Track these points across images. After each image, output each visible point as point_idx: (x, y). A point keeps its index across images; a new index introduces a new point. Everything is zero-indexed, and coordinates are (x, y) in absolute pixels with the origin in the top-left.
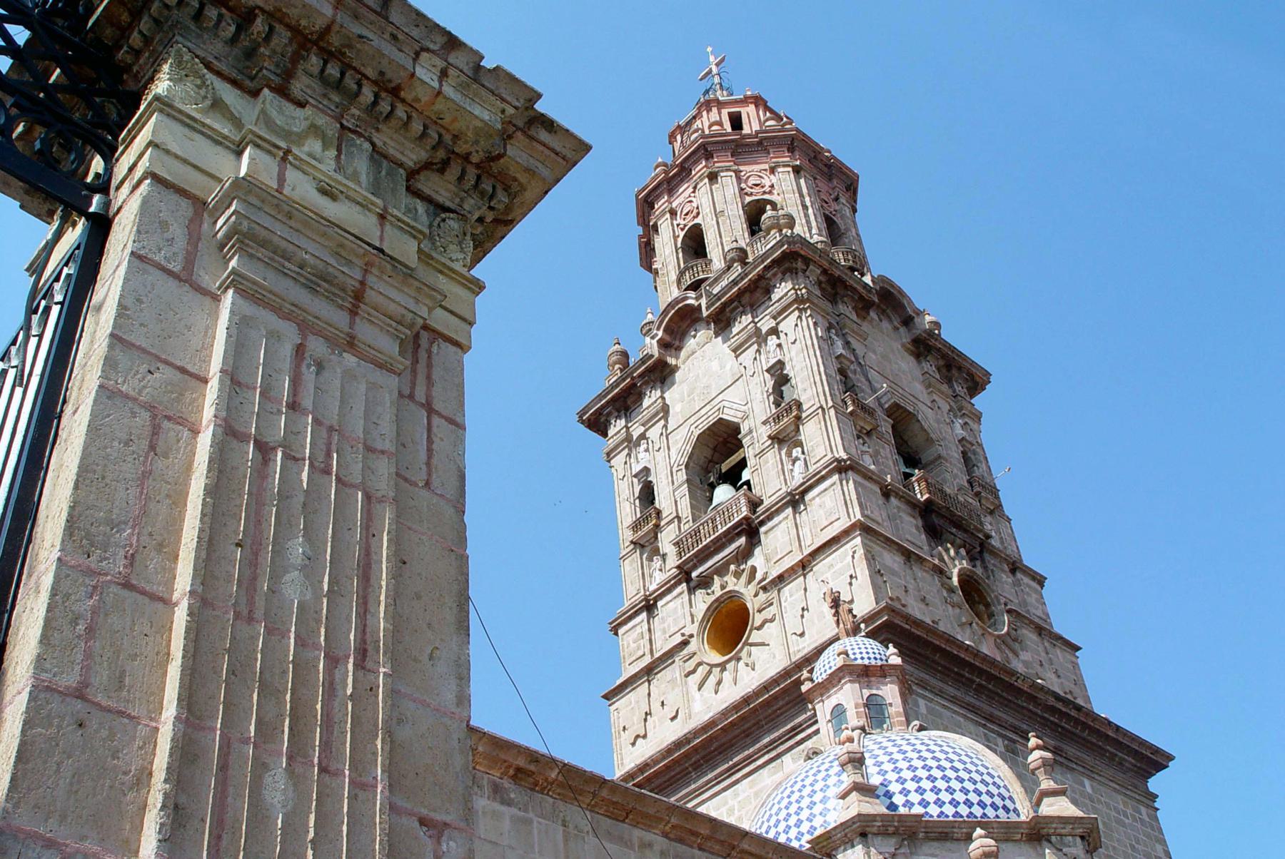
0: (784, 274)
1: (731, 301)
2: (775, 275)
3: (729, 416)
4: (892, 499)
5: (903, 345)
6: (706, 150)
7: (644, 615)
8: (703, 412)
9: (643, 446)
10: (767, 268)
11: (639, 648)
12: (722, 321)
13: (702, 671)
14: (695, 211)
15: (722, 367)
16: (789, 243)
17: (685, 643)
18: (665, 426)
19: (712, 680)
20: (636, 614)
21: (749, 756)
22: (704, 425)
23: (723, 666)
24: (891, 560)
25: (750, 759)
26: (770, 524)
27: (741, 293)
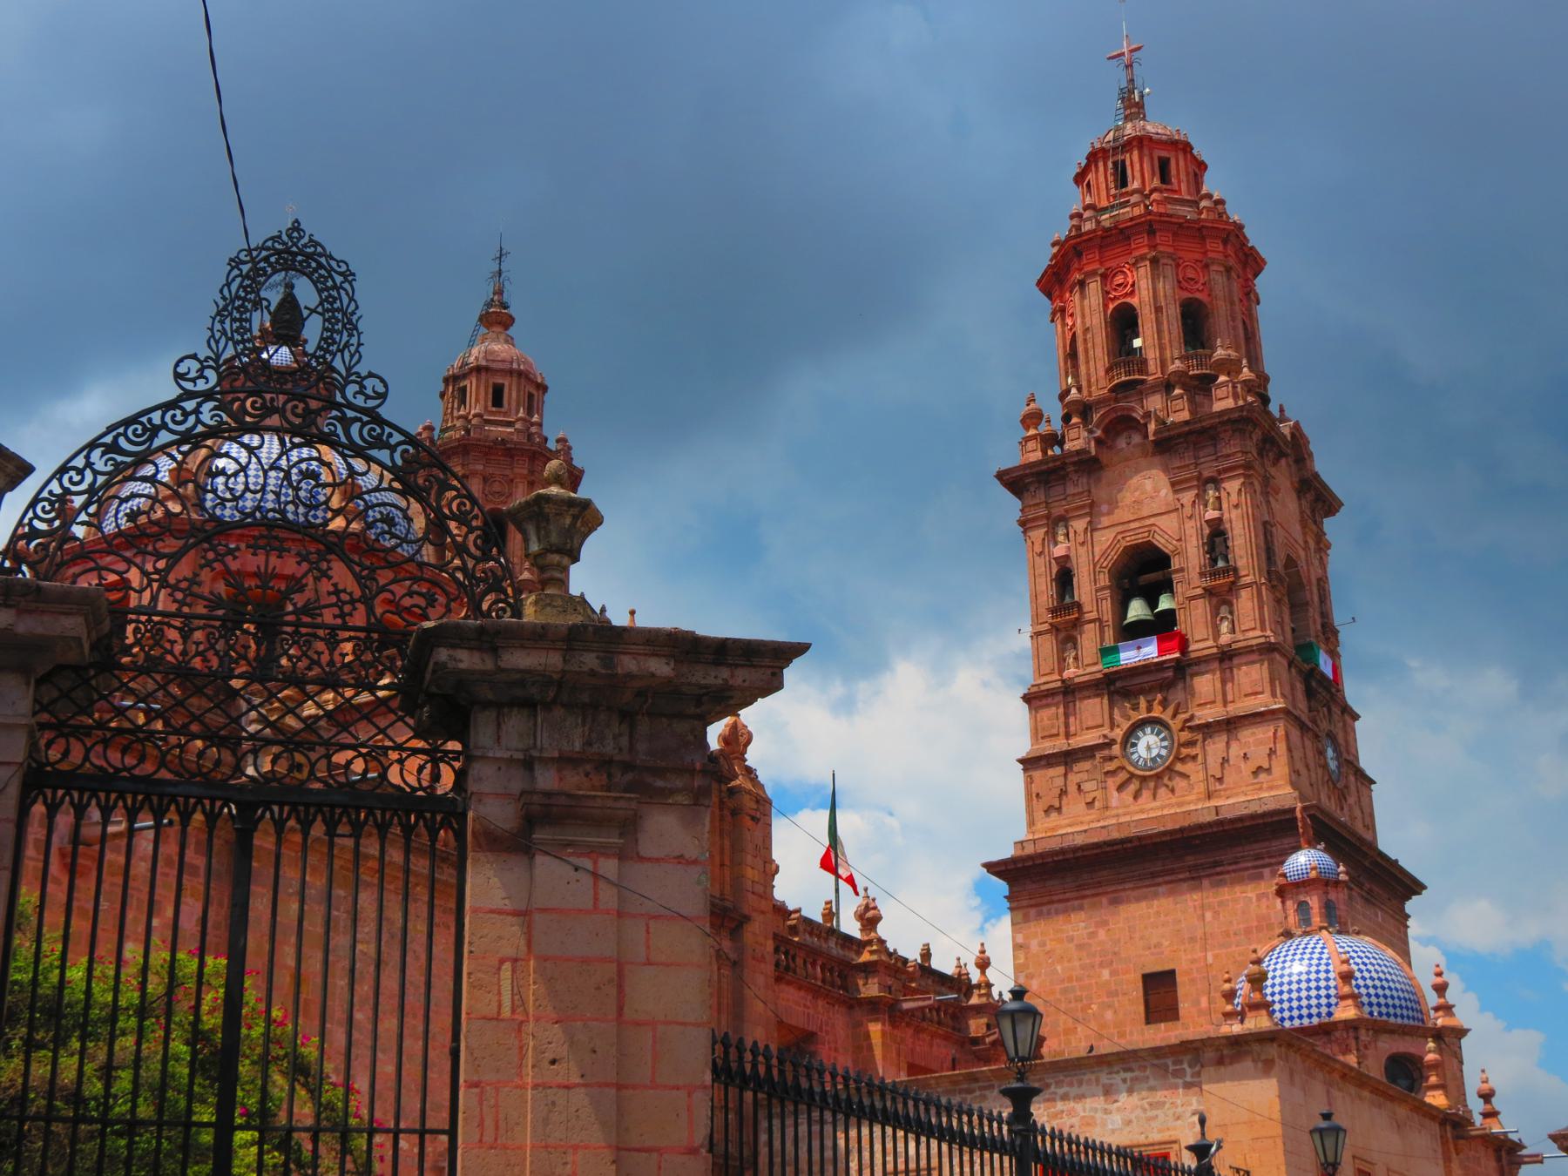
0: (1234, 431)
1: (1179, 435)
2: (1225, 431)
3: (1160, 541)
5: (1292, 483)
6: (1151, 226)
7: (1059, 698)
8: (1133, 525)
9: (1061, 531)
11: (1053, 727)
13: (1123, 776)
14: (1128, 289)
15: (1157, 491)
16: (1248, 411)
17: (1109, 744)
19: (1133, 787)
20: (1053, 694)
21: (1173, 869)
22: (1131, 540)
23: (1144, 779)
24: (1295, 734)
25: (1172, 872)
27: (1190, 433)
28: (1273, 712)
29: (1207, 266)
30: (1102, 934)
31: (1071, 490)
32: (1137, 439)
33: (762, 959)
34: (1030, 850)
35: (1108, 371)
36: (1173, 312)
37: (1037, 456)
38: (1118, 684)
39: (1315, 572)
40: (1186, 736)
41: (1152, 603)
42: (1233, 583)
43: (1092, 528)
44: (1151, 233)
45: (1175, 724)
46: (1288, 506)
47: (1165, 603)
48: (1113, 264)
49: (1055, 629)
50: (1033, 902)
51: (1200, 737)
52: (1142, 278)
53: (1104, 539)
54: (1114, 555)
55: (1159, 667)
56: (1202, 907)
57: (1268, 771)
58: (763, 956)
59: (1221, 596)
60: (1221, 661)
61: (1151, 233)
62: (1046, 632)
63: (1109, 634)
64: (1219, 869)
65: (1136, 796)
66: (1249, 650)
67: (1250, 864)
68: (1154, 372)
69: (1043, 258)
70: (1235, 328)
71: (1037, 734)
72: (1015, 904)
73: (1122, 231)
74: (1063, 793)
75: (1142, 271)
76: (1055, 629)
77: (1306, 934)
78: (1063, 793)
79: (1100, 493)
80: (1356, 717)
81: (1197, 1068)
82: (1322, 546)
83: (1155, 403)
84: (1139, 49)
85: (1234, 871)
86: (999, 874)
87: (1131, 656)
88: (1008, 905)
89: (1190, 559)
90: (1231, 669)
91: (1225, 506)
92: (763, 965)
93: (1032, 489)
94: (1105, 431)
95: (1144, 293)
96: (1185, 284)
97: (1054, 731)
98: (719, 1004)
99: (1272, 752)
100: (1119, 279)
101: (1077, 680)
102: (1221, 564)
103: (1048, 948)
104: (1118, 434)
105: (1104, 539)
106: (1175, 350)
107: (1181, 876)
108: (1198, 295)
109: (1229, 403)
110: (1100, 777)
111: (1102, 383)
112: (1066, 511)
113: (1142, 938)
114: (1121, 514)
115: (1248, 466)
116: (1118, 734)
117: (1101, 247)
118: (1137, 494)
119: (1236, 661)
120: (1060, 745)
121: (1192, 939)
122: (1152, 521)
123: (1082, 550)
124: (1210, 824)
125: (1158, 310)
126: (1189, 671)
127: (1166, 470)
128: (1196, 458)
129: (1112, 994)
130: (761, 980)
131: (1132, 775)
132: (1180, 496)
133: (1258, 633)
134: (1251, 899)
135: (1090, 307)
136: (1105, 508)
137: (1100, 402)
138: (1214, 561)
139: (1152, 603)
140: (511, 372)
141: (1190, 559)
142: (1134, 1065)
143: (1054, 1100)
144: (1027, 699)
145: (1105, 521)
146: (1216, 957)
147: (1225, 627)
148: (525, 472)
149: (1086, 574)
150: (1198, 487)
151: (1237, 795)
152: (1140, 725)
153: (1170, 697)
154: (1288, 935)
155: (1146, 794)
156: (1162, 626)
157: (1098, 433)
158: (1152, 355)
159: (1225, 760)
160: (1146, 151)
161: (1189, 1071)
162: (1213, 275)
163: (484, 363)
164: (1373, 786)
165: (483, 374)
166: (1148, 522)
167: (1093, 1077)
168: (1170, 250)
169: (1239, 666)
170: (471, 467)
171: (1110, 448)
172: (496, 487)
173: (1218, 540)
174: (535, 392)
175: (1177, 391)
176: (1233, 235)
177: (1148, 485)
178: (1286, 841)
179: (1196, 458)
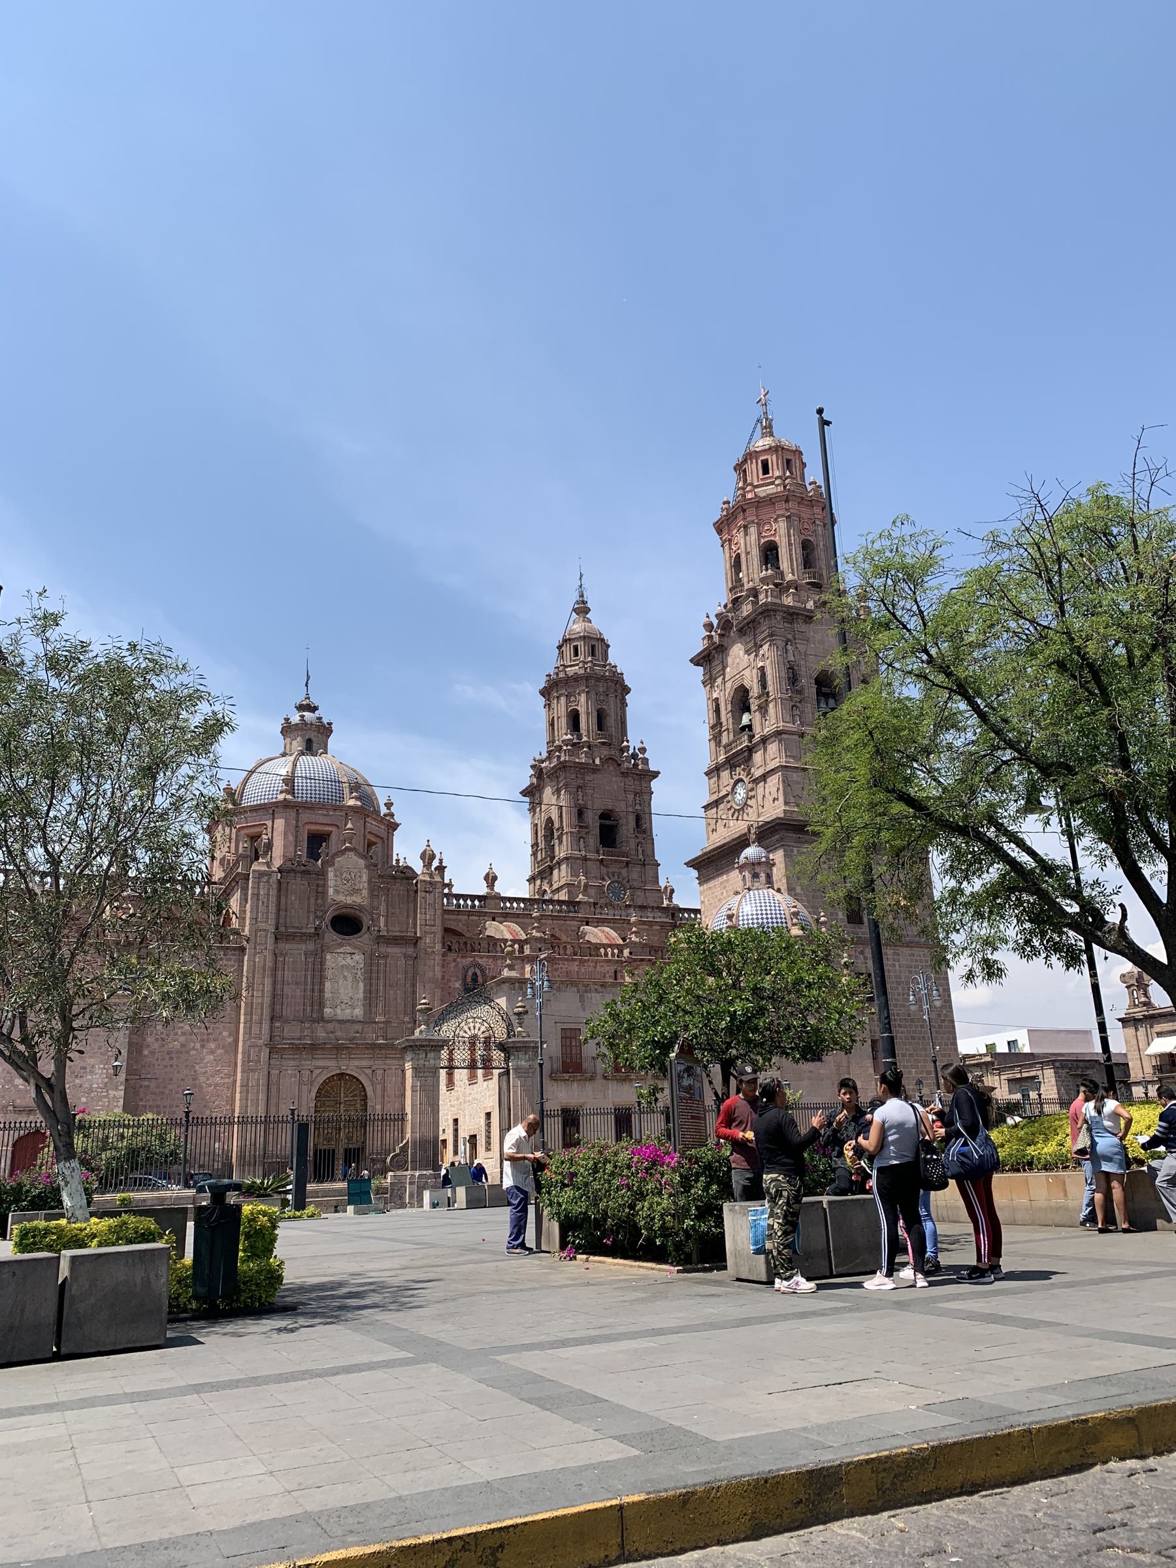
3: (747, 684)
12: (742, 631)
13: (733, 810)
17: (727, 795)
18: (724, 679)
23: (739, 811)
27: (748, 624)
36: (755, 552)
43: (724, 682)
44: (744, 511)
89: (755, 690)
99: (778, 789)
108: (773, 538)
125: (747, 553)
141: (755, 690)
158: (745, 580)
159: (764, 796)
174: (596, 643)
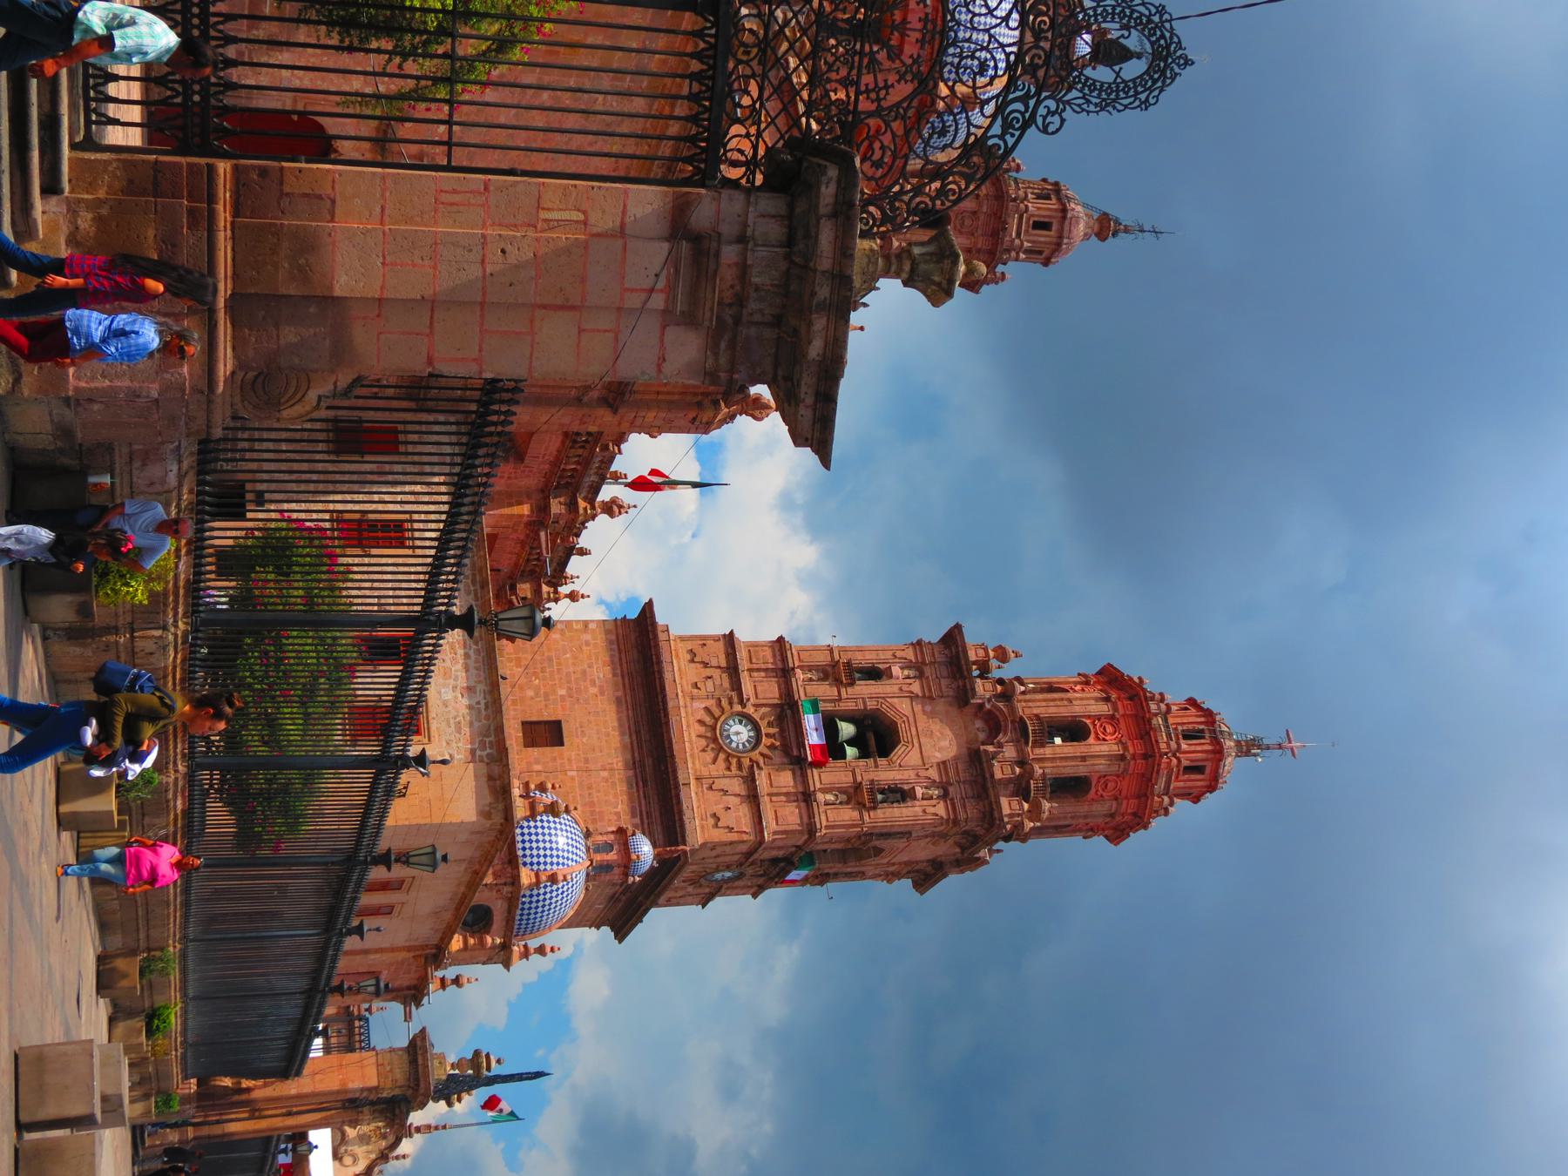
0: (983, 813)
1: (982, 770)
2: (984, 806)
3: (899, 750)
4: (794, 849)
6: (1151, 756)
7: (780, 665)
8: (913, 729)
9: (912, 673)
10: (991, 804)
11: (758, 659)
13: (717, 712)
14: (1101, 736)
15: (940, 750)
17: (742, 702)
19: (708, 720)
22: (902, 727)
23: (714, 728)
24: (744, 848)
25: (640, 748)
26: (798, 773)
28: (762, 832)
29: (1116, 799)
30: (594, 690)
31: (944, 682)
32: (982, 736)
33: (582, 422)
34: (662, 636)
35: (1037, 716)
36: (1081, 770)
37: (972, 656)
38: (789, 712)
39: (870, 871)
40: (746, 762)
41: (851, 742)
42: (864, 806)
43: (913, 697)
44: (1145, 756)
45: (755, 755)
46: (922, 852)
47: (851, 752)
48: (1122, 725)
49: (835, 664)
50: (621, 637)
51: (745, 774)
52: (1110, 747)
53: (904, 706)
54: (891, 714)
55: (801, 745)
56: (611, 769)
57: (716, 826)
58: (584, 423)
59: (855, 795)
60: (803, 794)
61: (1145, 756)
62: (832, 657)
63: (829, 707)
64: (641, 784)
65: (701, 722)
66: (811, 816)
67: (644, 809)
68: (1033, 752)
69: (1131, 670)
70: (1065, 818)
71: (753, 647)
72: (619, 623)
73: (1148, 733)
74: (706, 665)
75: (1115, 747)
76: (835, 664)
77: (588, 849)
78: (706, 665)
79: (941, 706)
80: (755, 896)
81: (485, 759)
82: (890, 877)
83: (1010, 752)
84: (1294, 755)
85: (639, 796)
86: (644, 609)
87: (810, 722)
88: (619, 618)
89: (885, 773)
90: (797, 801)
91: (925, 802)
92: (578, 422)
93: (946, 652)
94: (990, 712)
95: (1097, 748)
96: (1102, 781)
97: (754, 661)
98: (548, 386)
99: (731, 829)
100: (1109, 729)
101: (793, 680)
102: (880, 797)
103: (584, 648)
104: (987, 722)
105: (904, 706)
106: (1051, 770)
107: (636, 755)
108: (1093, 790)
109: (1006, 810)
110: (717, 694)
111: (1028, 711)
112: (928, 678)
113: (590, 722)
114: (922, 720)
115: (956, 822)
116: (750, 710)
117: (1136, 716)
118: (938, 734)
119: (803, 805)
120: (743, 664)
121: (587, 761)
122: (916, 745)
123: (896, 689)
124: (676, 778)
125: (1084, 758)
126: (797, 767)
127: (956, 758)
128: (964, 782)
129: (546, 695)
130: (566, 420)
131: (717, 720)
132: (935, 767)
133: (824, 823)
134: (617, 807)
135: (1088, 704)
136: (928, 708)
137: (1012, 709)
138: (882, 792)
139: (851, 742)
140: (1061, 237)
141: (885, 773)
142: (490, 710)
143: (465, 647)
144: (781, 640)
145: (918, 708)
146: (573, 778)
147: (830, 797)
148: (979, 246)
149: (877, 691)
150: (941, 782)
151: (699, 800)
152: (756, 728)
153: (777, 752)
154: (588, 835)
155: (702, 729)
156: (833, 749)
157: (988, 706)
158: (1047, 751)
159: (725, 792)
160: (1210, 756)
161: (485, 753)
162: (1108, 804)
163: (1069, 215)
164: (700, 906)
165: (1060, 215)
166: (915, 741)
167: (482, 678)
168: (1130, 771)
169: (798, 807)
170: (985, 202)
171: (976, 715)
172: (968, 222)
173: (899, 795)
174: (1044, 255)
175: (1018, 770)
176: (1139, 821)
177: (945, 743)
178: (661, 837)
179: (964, 782)
